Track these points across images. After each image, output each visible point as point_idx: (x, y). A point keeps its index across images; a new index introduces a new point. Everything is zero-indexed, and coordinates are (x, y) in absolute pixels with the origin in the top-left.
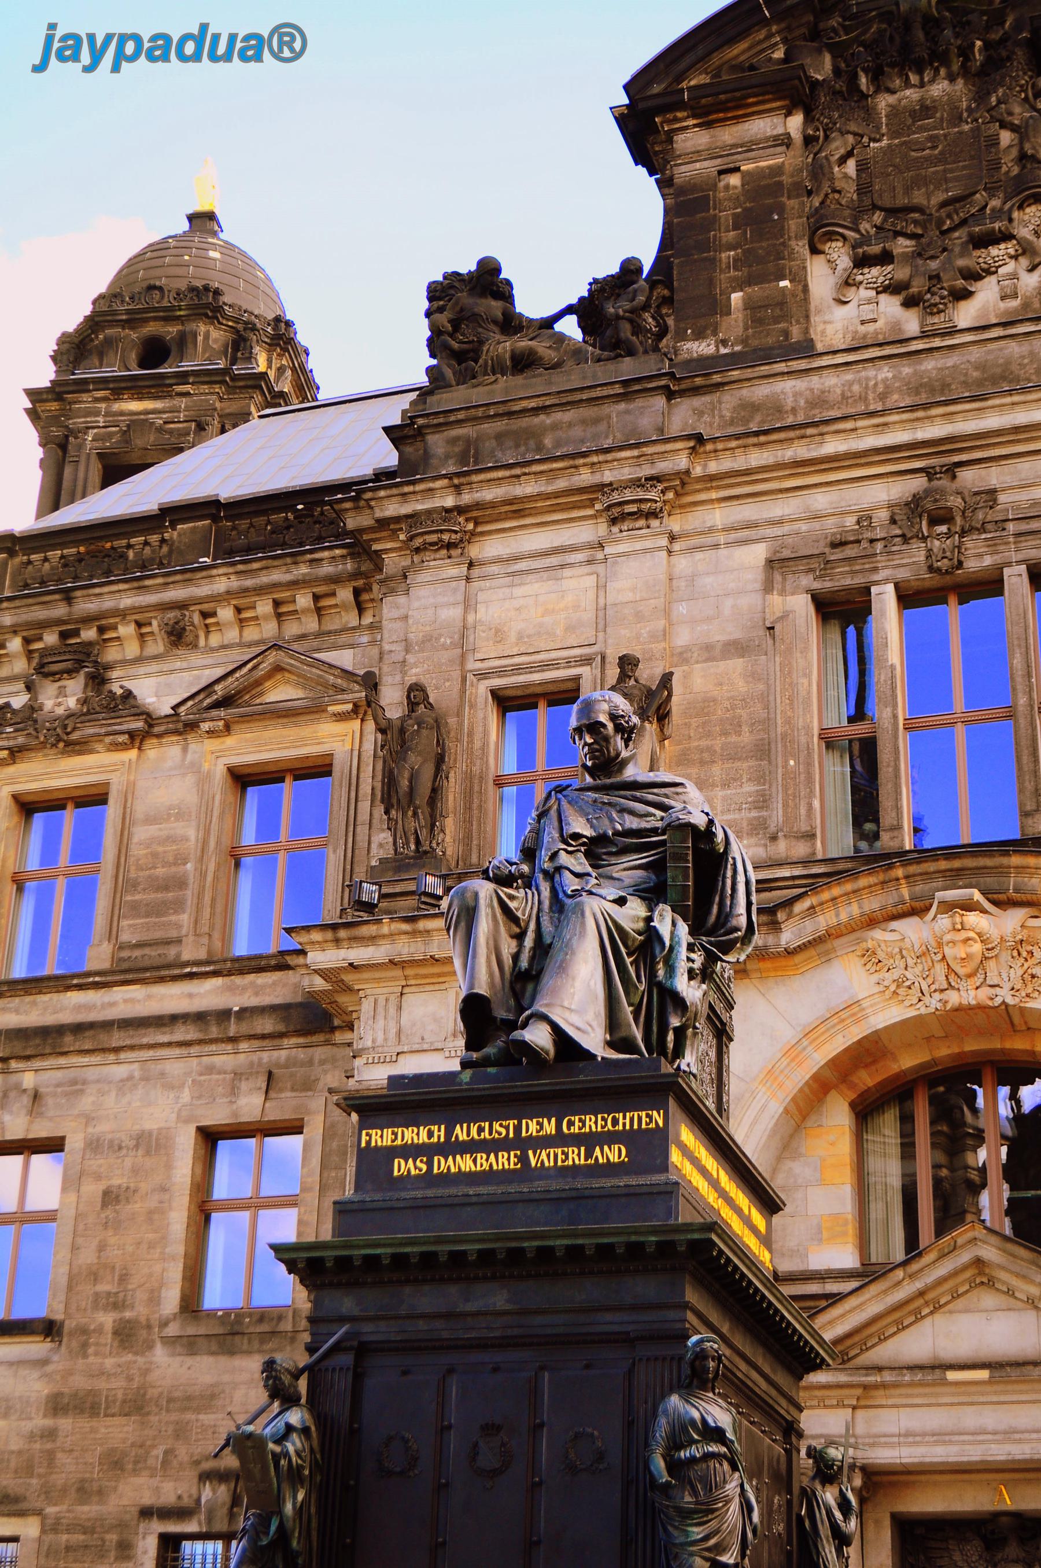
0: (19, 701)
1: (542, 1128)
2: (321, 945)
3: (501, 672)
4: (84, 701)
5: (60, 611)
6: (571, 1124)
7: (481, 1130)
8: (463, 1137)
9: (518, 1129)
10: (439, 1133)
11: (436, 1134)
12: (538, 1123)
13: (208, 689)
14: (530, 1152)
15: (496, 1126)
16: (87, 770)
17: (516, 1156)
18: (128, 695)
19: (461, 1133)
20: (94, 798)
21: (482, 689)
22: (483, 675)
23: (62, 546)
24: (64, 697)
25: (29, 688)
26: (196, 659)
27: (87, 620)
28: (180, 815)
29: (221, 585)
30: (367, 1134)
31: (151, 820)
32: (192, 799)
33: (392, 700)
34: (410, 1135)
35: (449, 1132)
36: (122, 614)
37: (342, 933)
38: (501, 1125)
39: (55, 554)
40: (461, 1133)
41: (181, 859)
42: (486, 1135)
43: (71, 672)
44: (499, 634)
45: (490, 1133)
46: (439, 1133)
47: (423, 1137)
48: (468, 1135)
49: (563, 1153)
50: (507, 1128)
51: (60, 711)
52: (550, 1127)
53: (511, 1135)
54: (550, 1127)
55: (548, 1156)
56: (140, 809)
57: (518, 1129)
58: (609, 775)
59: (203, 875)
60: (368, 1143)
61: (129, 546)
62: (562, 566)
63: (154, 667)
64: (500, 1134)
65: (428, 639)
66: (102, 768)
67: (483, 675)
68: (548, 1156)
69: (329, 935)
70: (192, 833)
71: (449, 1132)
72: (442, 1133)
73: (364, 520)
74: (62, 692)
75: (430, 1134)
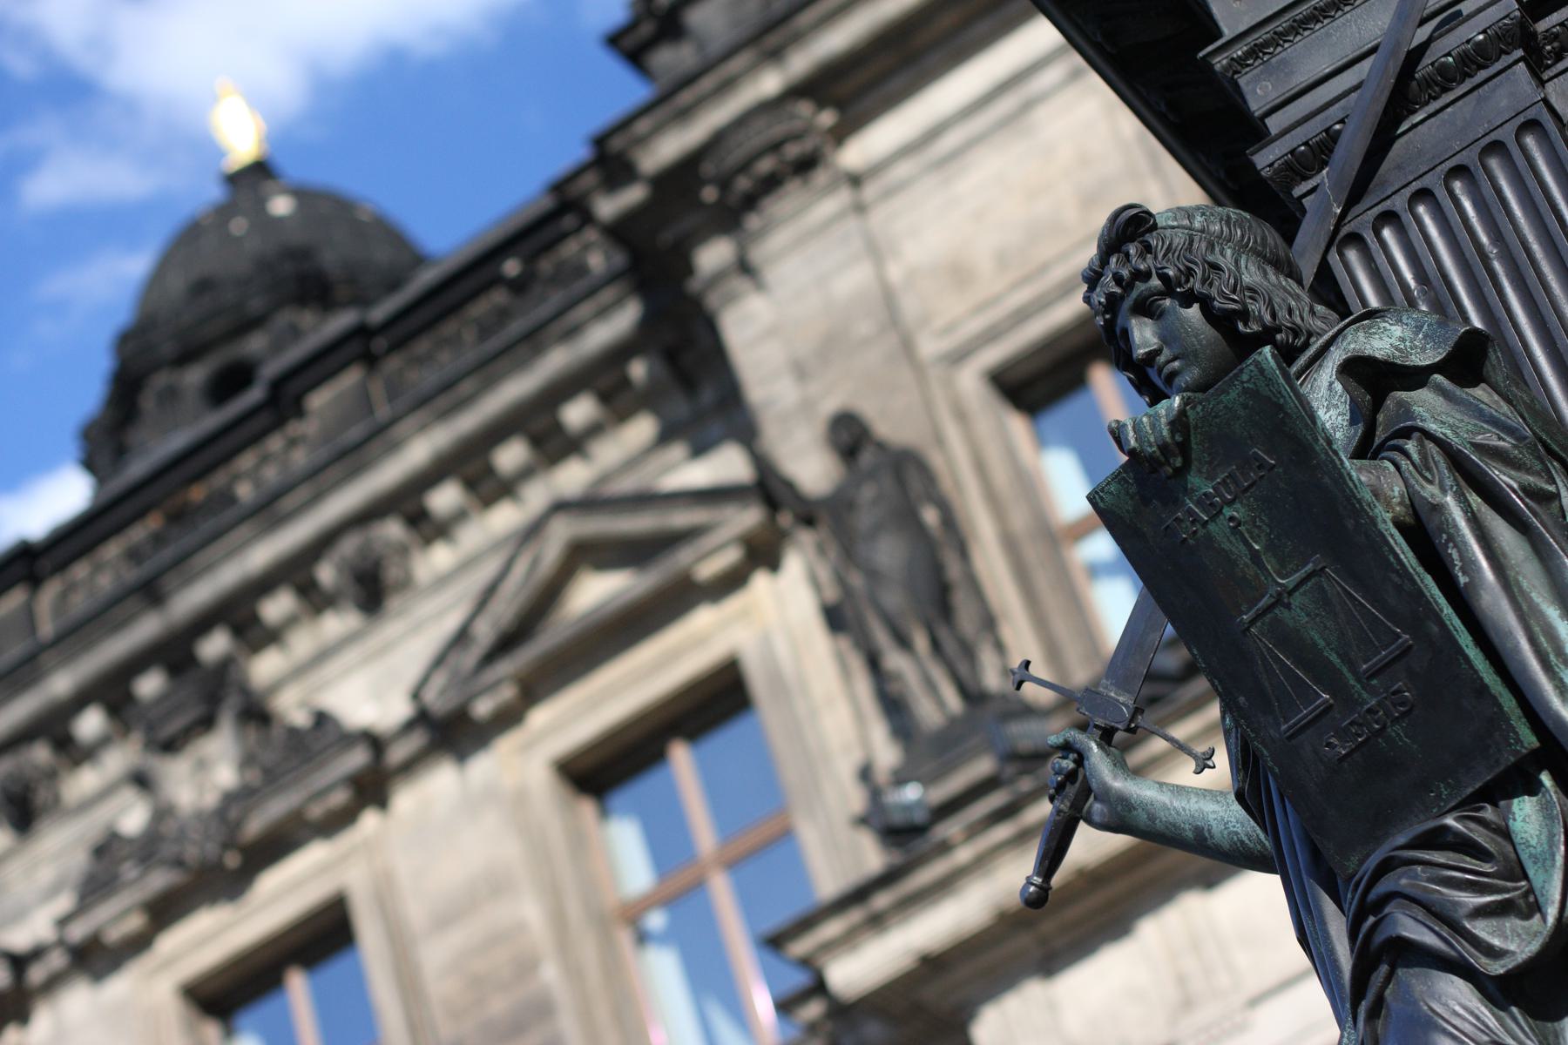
0: (133, 818)
2: (847, 941)
3: (991, 335)
4: (247, 761)
5: (147, 628)
13: (462, 637)
16: (296, 885)
18: (322, 719)
20: (325, 935)
21: (970, 381)
22: (958, 357)
23: (118, 529)
24: (208, 773)
25: (141, 781)
26: (426, 607)
27: (203, 623)
28: (495, 886)
29: (418, 452)
31: (445, 920)
32: (508, 851)
33: (811, 468)
36: (264, 585)
37: (882, 900)
39: (112, 550)
41: (526, 966)
43: (206, 724)
44: (958, 274)
51: (211, 800)
56: (415, 912)
59: (574, 973)
61: (236, 478)
62: (1028, 106)
63: (351, 656)
65: (834, 344)
66: (323, 869)
67: (958, 357)
69: (855, 915)
70: (530, 912)
73: (633, 195)
74: (202, 765)
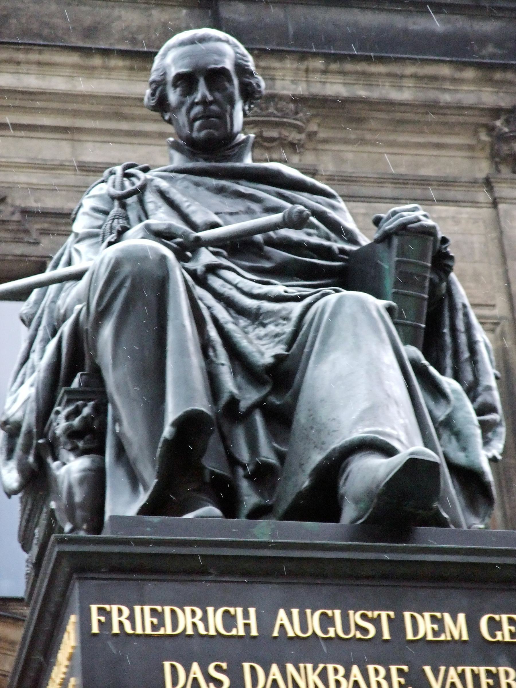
1: (442, 629)
6: (495, 626)
7: (326, 622)
8: (294, 630)
9: (396, 625)
10: (247, 621)
11: (240, 621)
12: (434, 619)
14: (428, 669)
15: (355, 617)
17: (400, 672)
19: (288, 622)
30: (101, 611)
34: (187, 620)
35: (266, 621)
38: (364, 617)
40: (288, 622)
42: (337, 630)
45: (346, 630)
46: (247, 621)
47: (216, 621)
48: (304, 627)
49: (489, 674)
50: (376, 622)
52: (457, 628)
53: (386, 636)
54: (457, 628)
55: (462, 676)
57: (396, 625)
58: (227, 158)
60: (105, 626)
64: (365, 631)
68: (462, 676)
71: (266, 621)
72: (253, 621)
75: (229, 620)
